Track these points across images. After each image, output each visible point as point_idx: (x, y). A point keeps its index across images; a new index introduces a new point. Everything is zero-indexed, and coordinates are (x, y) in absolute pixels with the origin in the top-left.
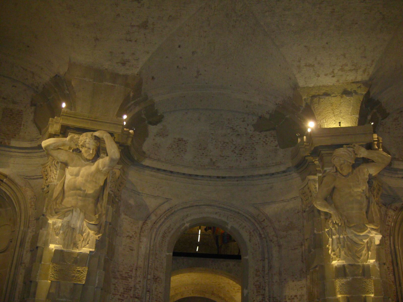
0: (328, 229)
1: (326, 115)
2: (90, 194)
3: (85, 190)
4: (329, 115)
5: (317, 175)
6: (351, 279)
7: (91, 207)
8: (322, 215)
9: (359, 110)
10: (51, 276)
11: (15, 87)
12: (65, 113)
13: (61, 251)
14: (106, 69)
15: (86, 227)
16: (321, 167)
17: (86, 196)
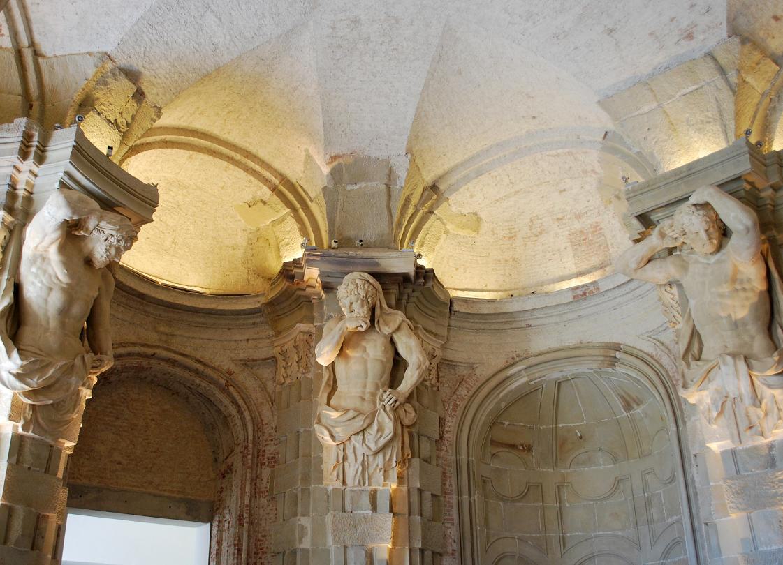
2: (743, 319)
3: (730, 316)
7: (759, 343)
10: (730, 507)
11: (565, 190)
12: (630, 193)
13: (733, 453)
14: (666, 68)
15: (761, 386)
17: (736, 325)
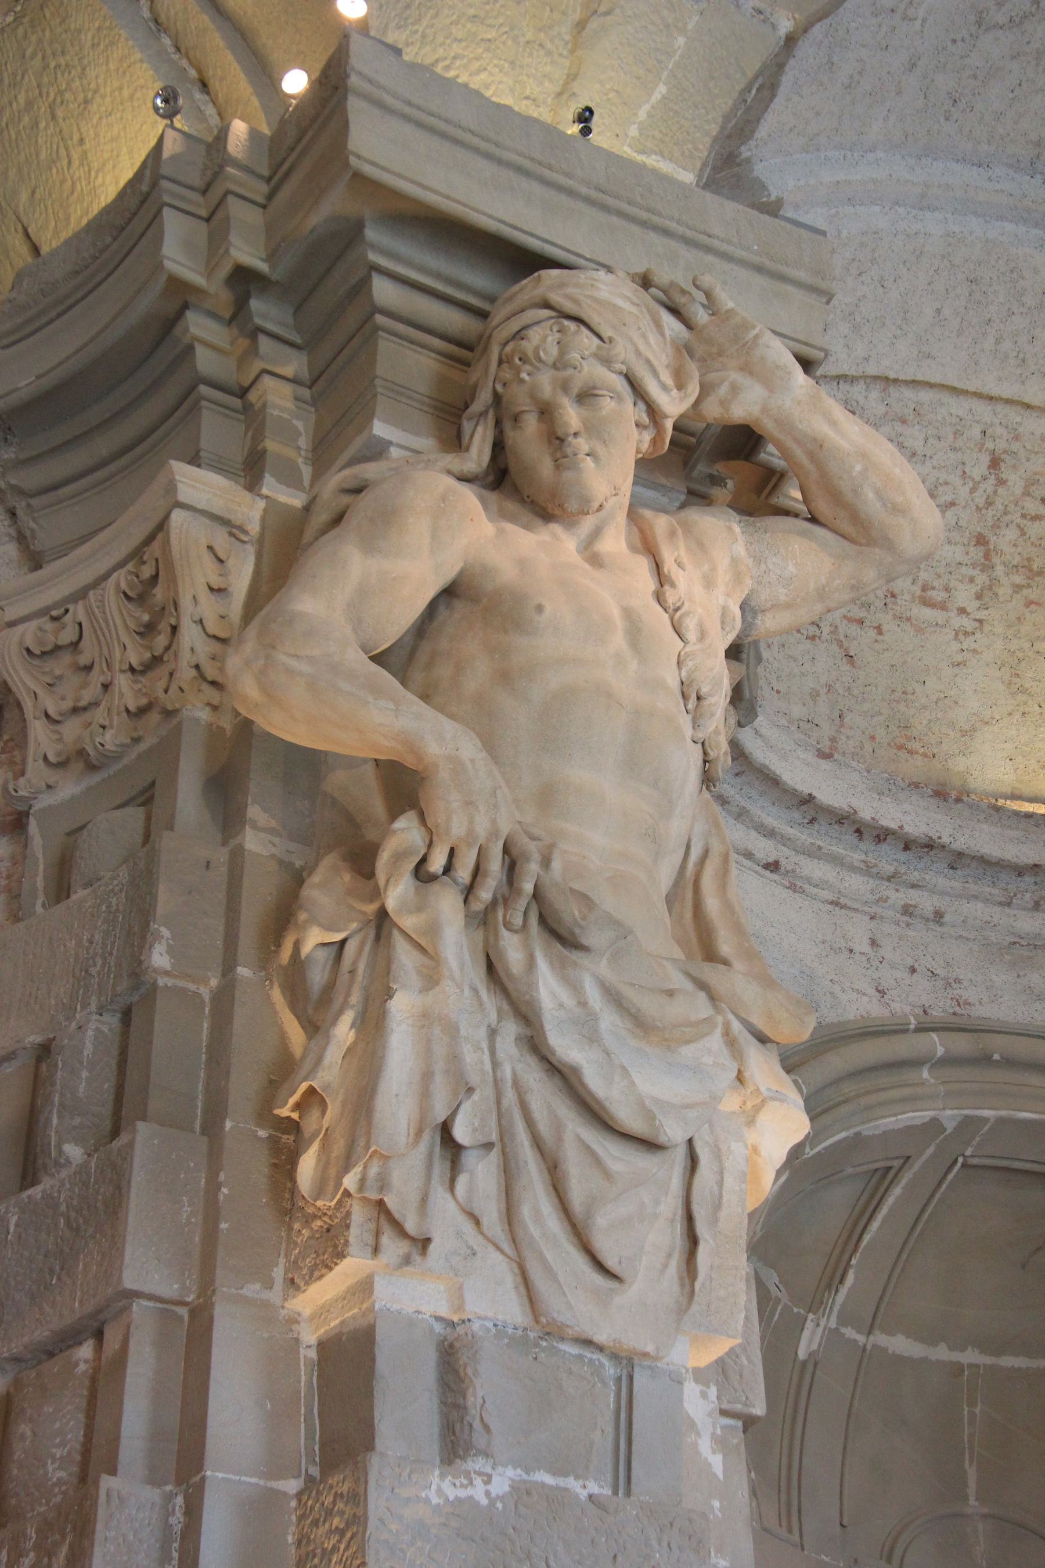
0: (338, 937)
1: (457, 49)
4: (476, 65)
5: (265, 491)
6: (500, 1485)
8: (255, 827)
9: (708, 140)
16: (303, 442)
